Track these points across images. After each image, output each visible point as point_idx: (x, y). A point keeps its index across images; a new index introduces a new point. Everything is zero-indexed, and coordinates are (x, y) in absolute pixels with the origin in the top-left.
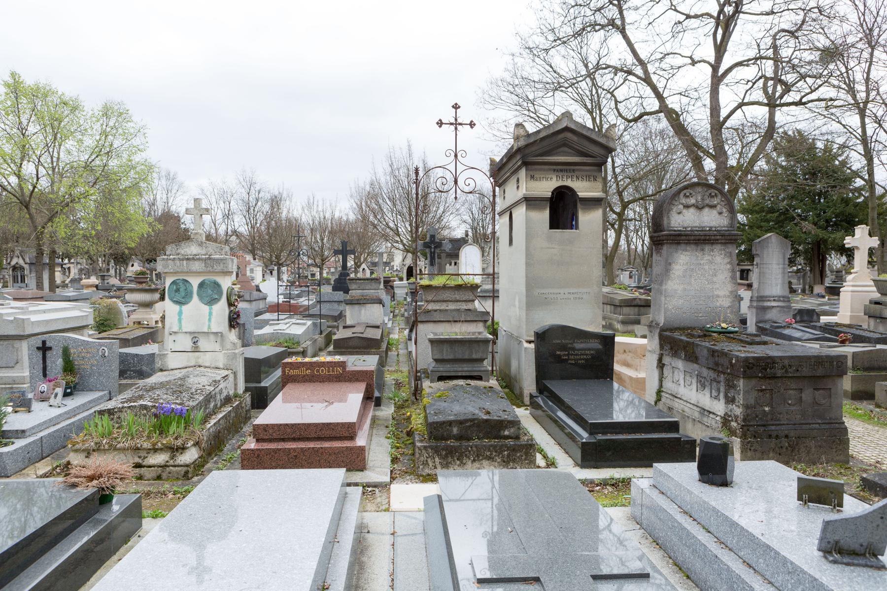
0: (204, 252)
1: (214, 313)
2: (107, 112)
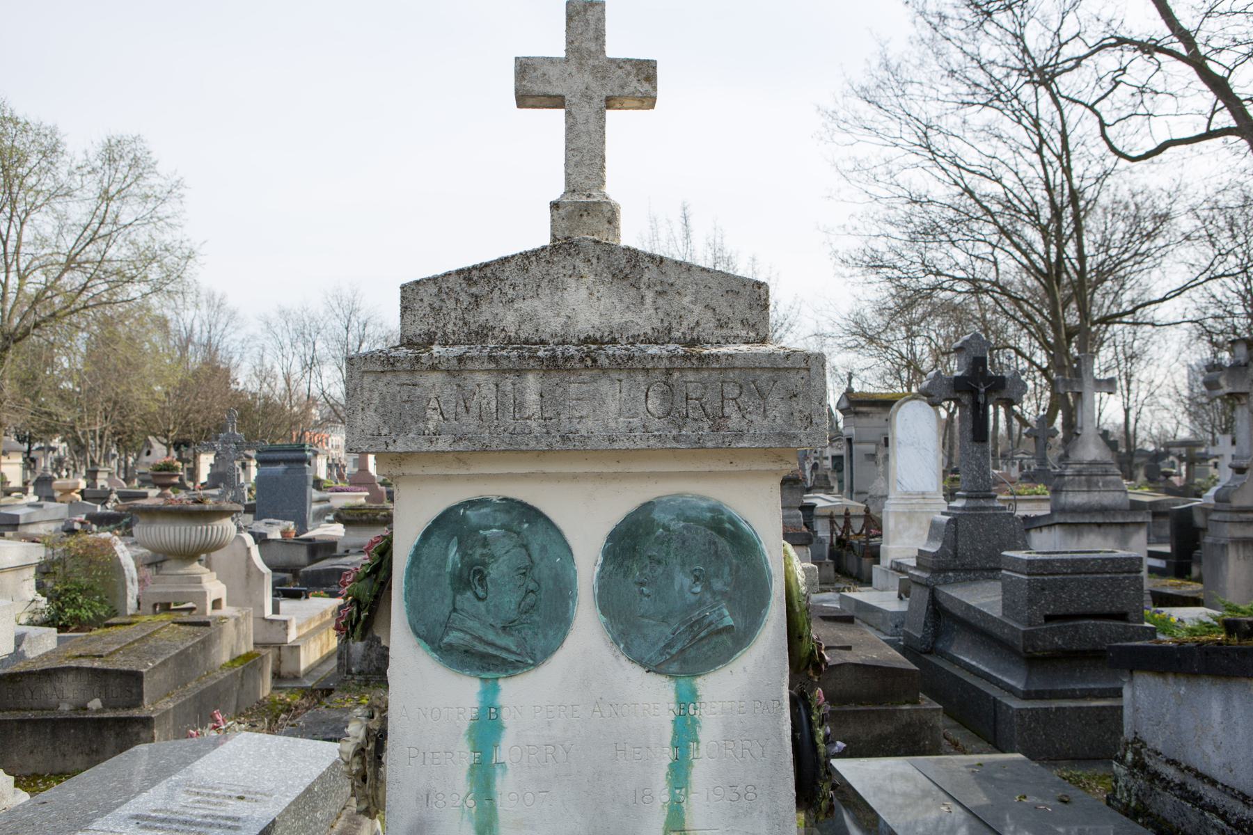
0: (644, 320)
1: (709, 730)
2: (111, 154)
